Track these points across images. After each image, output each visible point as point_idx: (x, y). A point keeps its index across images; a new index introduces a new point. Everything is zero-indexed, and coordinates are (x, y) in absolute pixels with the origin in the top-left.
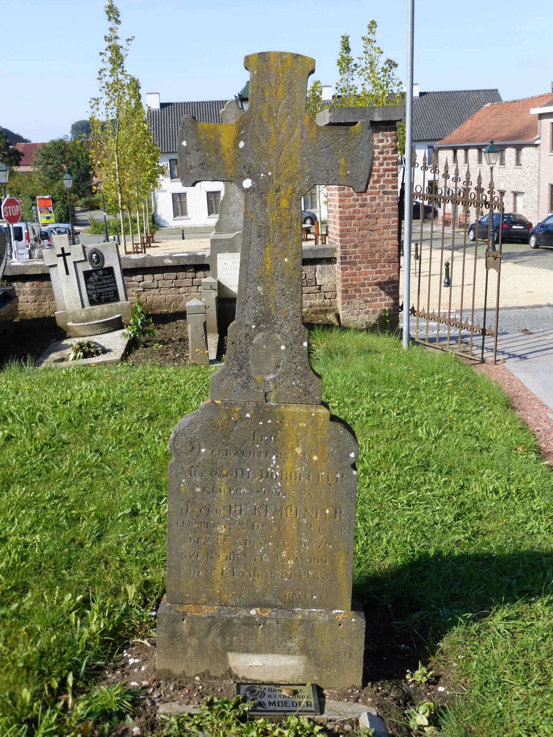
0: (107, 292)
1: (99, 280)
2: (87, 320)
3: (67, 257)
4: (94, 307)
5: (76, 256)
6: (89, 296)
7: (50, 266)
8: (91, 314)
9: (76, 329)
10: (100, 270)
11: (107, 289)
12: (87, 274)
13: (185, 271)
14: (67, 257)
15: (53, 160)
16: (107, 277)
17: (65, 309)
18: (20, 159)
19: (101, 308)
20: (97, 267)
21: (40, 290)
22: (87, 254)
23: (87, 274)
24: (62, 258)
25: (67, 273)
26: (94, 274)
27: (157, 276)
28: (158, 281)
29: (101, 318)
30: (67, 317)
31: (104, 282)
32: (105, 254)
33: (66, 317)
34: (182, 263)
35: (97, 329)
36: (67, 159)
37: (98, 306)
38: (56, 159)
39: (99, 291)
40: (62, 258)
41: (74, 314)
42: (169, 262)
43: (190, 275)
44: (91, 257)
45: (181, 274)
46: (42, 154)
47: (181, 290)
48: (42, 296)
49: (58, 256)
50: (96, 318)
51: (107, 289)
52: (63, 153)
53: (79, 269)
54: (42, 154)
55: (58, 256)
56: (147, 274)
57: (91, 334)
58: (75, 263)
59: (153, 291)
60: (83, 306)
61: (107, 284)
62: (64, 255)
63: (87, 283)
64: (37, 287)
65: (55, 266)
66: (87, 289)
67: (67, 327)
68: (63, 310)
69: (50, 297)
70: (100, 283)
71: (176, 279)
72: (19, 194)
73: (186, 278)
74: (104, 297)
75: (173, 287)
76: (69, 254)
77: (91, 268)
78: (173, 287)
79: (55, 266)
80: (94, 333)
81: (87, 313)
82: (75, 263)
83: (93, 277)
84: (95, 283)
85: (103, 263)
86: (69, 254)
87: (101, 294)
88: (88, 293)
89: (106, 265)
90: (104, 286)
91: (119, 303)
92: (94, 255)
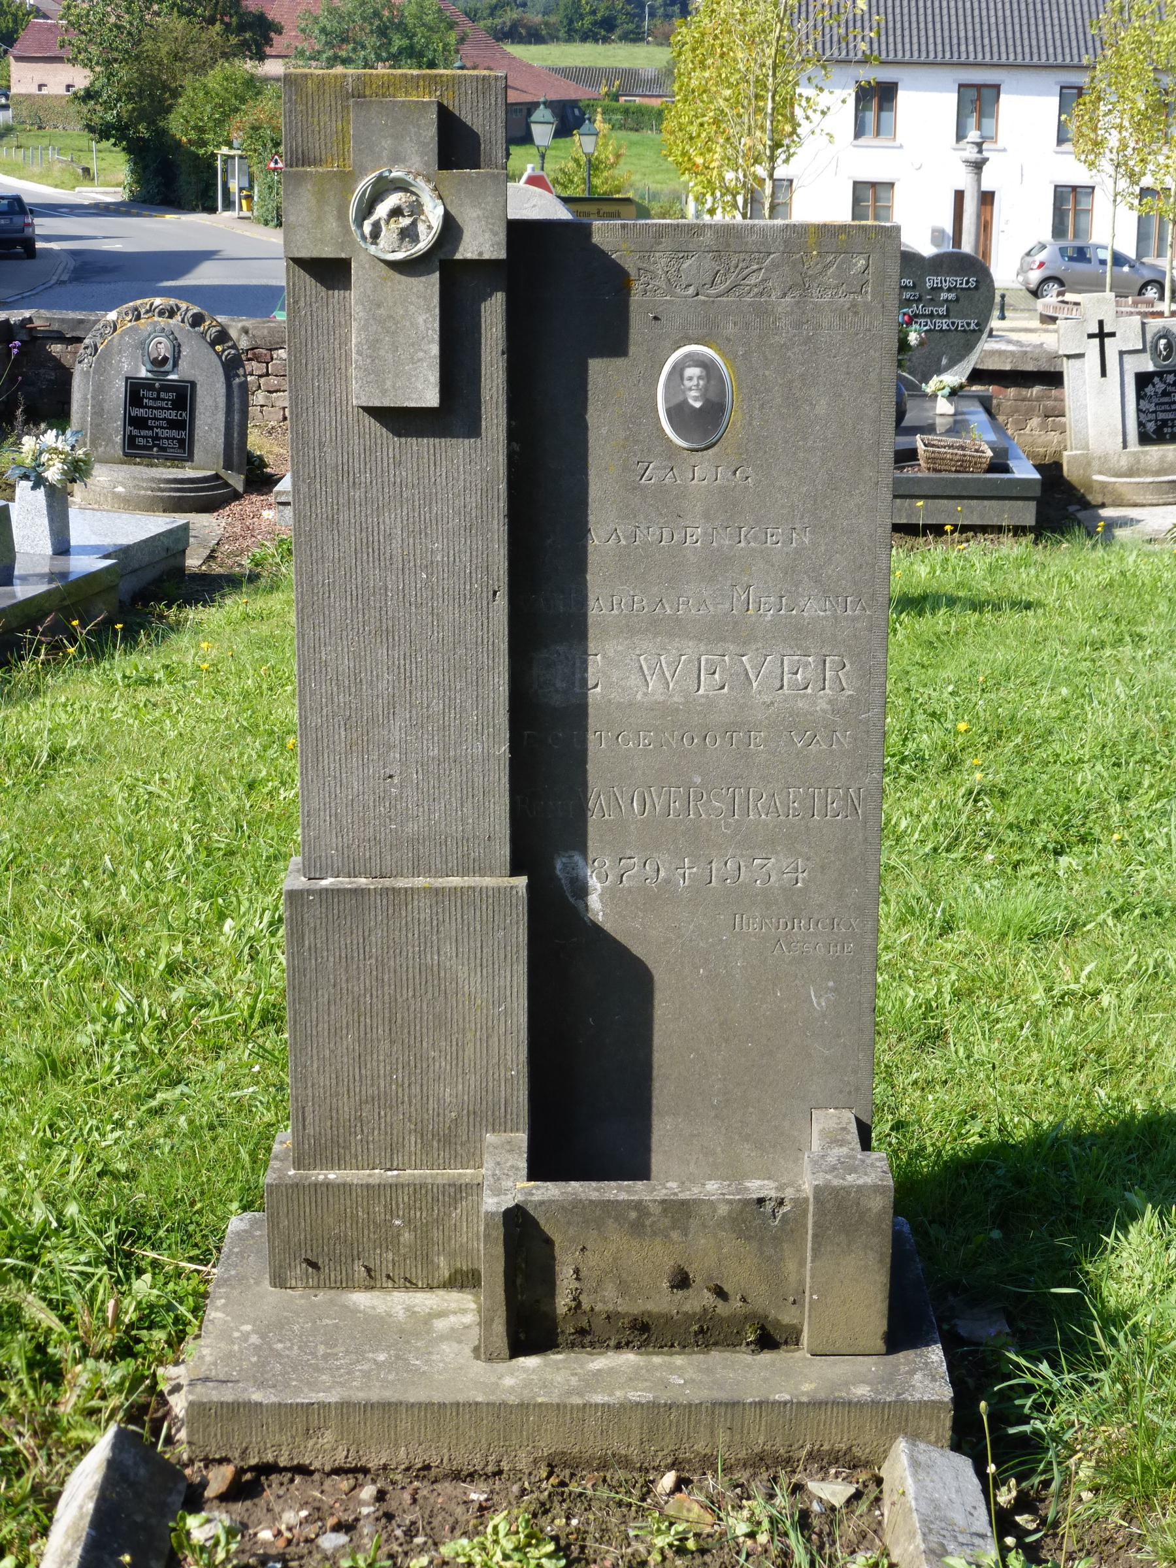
1: (1165, 393)
2: (1130, 473)
3: (1107, 340)
4: (1147, 448)
6: (1140, 424)
7: (1069, 357)
8: (1138, 462)
9: (1123, 490)
10: (1169, 372)
12: (1143, 380)
14: (1107, 340)
15: (354, 50)
17: (1086, 447)
18: (269, 41)
20: (1165, 366)
22: (1149, 338)
23: (1143, 380)
24: (1096, 341)
25: (1104, 374)
26: (1156, 380)
29: (1158, 473)
30: (1089, 464)
33: (1087, 462)
35: (1167, 493)
36: (394, 50)
37: (1155, 448)
38: (364, 47)
39: (1161, 416)
40: (1097, 341)
41: (1104, 459)
44: (1155, 346)
46: (323, 30)
49: (1091, 336)
50: (1146, 472)
52: (382, 32)
53: (1126, 366)
54: (323, 30)
55: (1091, 336)
57: (1155, 502)
58: (1121, 353)
60: (1125, 447)
62: (1102, 335)
63: (1140, 396)
65: (1080, 356)
66: (1139, 410)
67: (1090, 485)
69: (1016, 422)
70: (1166, 399)
72: (277, 144)
74: (1170, 430)
76: (1113, 335)
77: (1150, 367)
79: (1080, 356)
80: (1161, 501)
81: (1132, 459)
82: (1121, 353)
83: (1154, 386)
84: (1155, 400)
86: (1113, 335)
87: (1164, 423)
88: (1138, 417)
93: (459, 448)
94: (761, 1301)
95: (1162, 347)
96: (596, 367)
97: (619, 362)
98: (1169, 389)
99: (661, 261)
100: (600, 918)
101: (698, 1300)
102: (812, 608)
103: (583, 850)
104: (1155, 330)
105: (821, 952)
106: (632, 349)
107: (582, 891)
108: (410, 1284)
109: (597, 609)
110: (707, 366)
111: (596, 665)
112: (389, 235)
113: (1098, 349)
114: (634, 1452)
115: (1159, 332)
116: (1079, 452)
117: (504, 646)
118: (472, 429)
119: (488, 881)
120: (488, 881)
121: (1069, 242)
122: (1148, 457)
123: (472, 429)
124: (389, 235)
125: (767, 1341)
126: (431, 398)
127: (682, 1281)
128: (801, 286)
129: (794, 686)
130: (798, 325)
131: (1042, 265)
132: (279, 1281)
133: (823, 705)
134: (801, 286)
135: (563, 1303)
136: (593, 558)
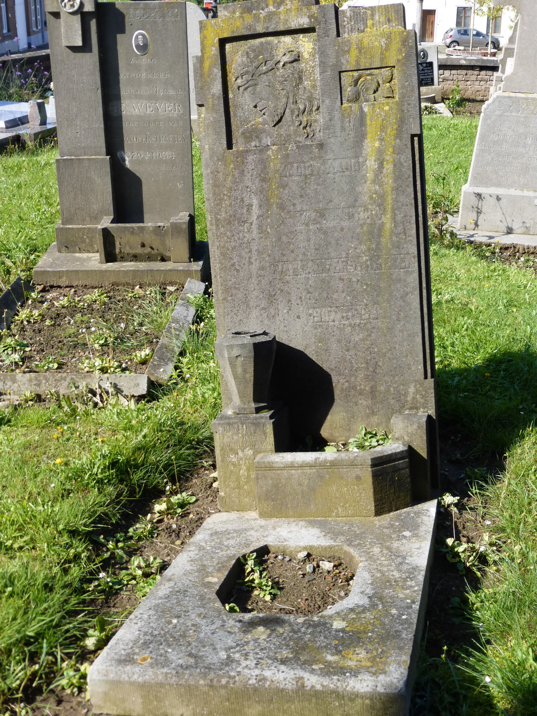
13: (473, 70)
27: (453, 72)
31: (426, 71)
32: (429, 53)
34: (472, 64)
42: (463, 62)
43: (476, 73)
45: (470, 72)
47: (469, 83)
56: (446, 69)
59: (449, 82)
89: (428, 61)
91: (433, 87)
93: (88, 55)
94: (161, 250)
96: (118, 36)
97: (123, 35)
99: (131, 11)
100: (129, 167)
101: (147, 250)
102: (171, 92)
103: (124, 151)
105: (179, 174)
106: (127, 32)
107: (124, 160)
108: (89, 252)
109: (123, 93)
110: (143, 35)
111: (123, 105)
112: (68, 6)
114: (131, 282)
117: (101, 101)
118: (90, 51)
119: (101, 157)
120: (101, 157)
121: (462, 28)
123: (90, 51)
124: (68, 6)
125: (163, 260)
126: (80, 43)
127: (143, 245)
128: (163, 16)
129: (169, 111)
130: (163, 25)
131: (451, 36)
132: (60, 251)
133: (175, 115)
134: (163, 16)
135: (117, 251)
136: (121, 81)
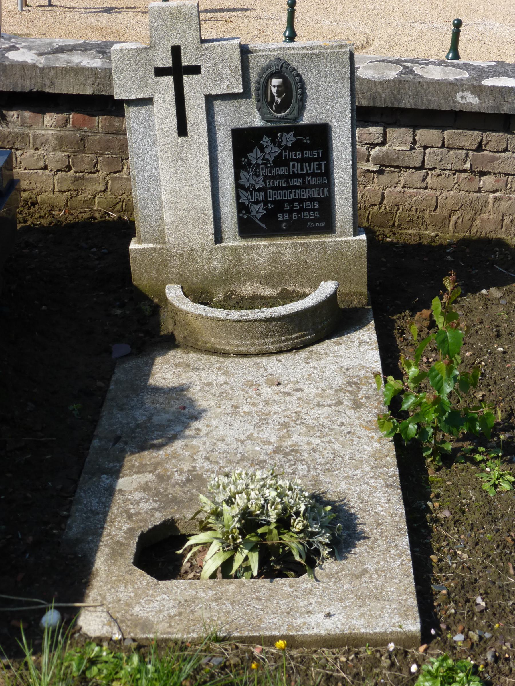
0: (301, 201)
1: (279, 162)
3: (187, 79)
4: (253, 242)
5: (217, 78)
6: (241, 207)
8: (239, 262)
9: (198, 325)
10: (287, 130)
11: (301, 193)
14: (187, 79)
16: (307, 155)
17: (161, 238)
19: (273, 250)
20: (280, 119)
21: (83, 140)
22: (254, 74)
24: (169, 80)
26: (266, 141)
28: (425, 148)
30: (165, 263)
31: (296, 169)
32: (310, 80)
35: (263, 336)
37: (264, 242)
39: (273, 195)
40: (169, 80)
44: (265, 86)
47: (487, 181)
48: (88, 157)
49: (160, 72)
51: (301, 193)
53: (219, 119)
55: (160, 72)
57: (243, 349)
58: (210, 99)
59: (405, 176)
60: (218, 237)
61: (303, 176)
63: (238, 167)
64: (76, 128)
65: (147, 102)
66: (238, 186)
68: (156, 241)
69: (109, 162)
70: (281, 171)
71: (479, 148)
73: (506, 150)
74: (287, 216)
75: (465, 171)
76: (196, 70)
77: (258, 122)
78: (465, 171)
79: (147, 102)
80: (253, 349)
81: (229, 259)
82: (210, 99)
83: (262, 150)
85: (301, 109)
86: (196, 70)
87: (279, 205)
88: (238, 197)
89: (307, 119)
90: (293, 182)
91: (330, 240)
92: (275, 82)
95: (274, 90)
98: (286, 154)
104: (265, 64)
113: (172, 92)
115: (269, 66)
116: (150, 245)
122: (254, 256)
